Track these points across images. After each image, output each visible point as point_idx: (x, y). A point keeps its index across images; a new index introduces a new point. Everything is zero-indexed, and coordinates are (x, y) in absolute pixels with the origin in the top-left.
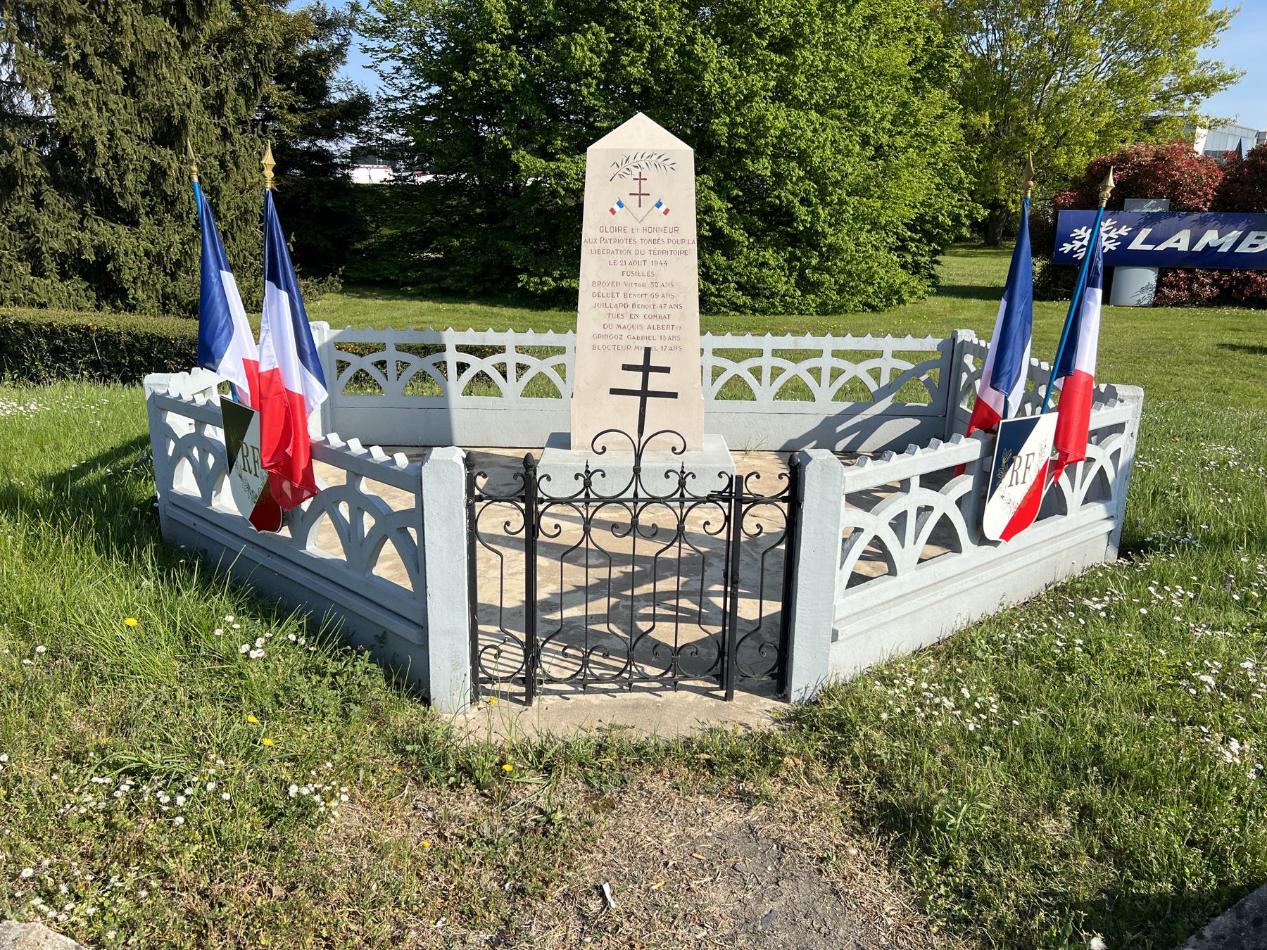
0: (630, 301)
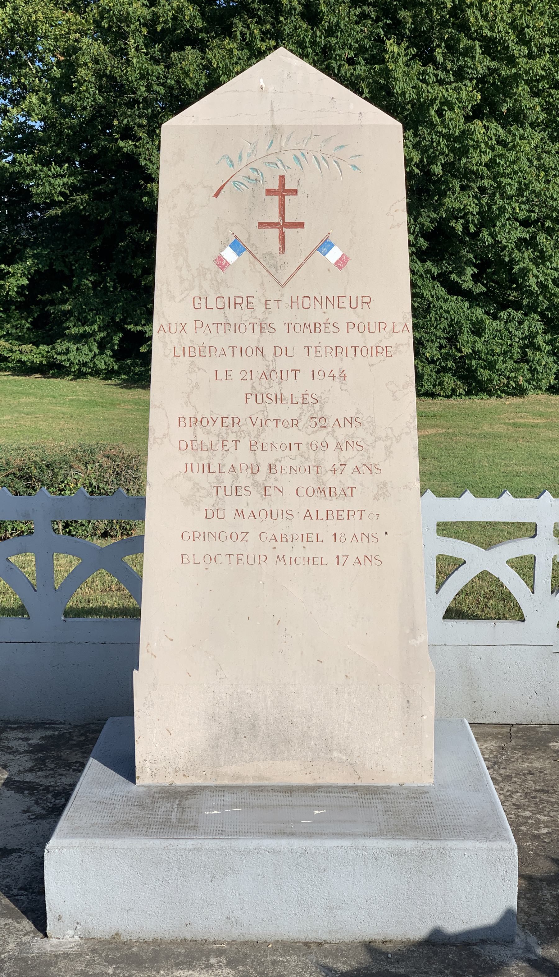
0: (264, 458)
